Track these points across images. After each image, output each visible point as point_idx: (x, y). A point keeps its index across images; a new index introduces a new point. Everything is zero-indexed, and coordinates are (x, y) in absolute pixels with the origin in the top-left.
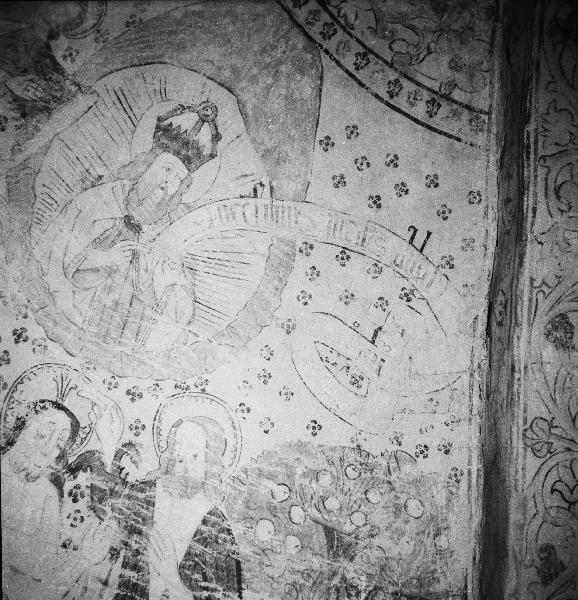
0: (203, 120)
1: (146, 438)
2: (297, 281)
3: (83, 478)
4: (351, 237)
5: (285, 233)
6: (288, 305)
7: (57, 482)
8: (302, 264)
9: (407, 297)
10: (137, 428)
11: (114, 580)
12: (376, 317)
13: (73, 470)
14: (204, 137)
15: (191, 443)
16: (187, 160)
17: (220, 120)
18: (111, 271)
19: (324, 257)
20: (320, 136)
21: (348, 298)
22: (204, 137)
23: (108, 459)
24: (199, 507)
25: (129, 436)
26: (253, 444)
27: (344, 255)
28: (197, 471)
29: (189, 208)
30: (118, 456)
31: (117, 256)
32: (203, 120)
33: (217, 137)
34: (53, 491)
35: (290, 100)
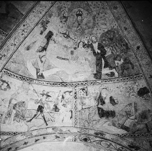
0: (79, 12)
1: (89, 40)
2: (96, 20)
3: (86, 46)
4: (98, 12)
5: (93, 16)
6: (97, 22)
7: (84, 47)
8: (96, 18)
9: (105, 14)
10: (88, 40)
11: (92, 52)
12: (104, 17)
13: (85, 46)
14: (81, 13)
15: (94, 38)
16: (81, 16)
17: (81, 10)
18: (80, 29)
19: (97, 16)
20: (90, 5)
21: (101, 17)
22: (81, 13)
23: (87, 44)
24: (97, 43)
25: (88, 41)
26: (99, 36)
27: (99, 14)
28: (95, 41)
29: (83, 20)
30: (88, 43)
31: (79, 27)
32: (79, 12)
33: (82, 12)
34: (84, 48)
35: (85, 4)
